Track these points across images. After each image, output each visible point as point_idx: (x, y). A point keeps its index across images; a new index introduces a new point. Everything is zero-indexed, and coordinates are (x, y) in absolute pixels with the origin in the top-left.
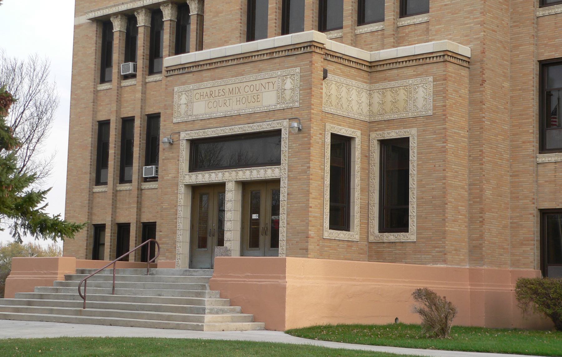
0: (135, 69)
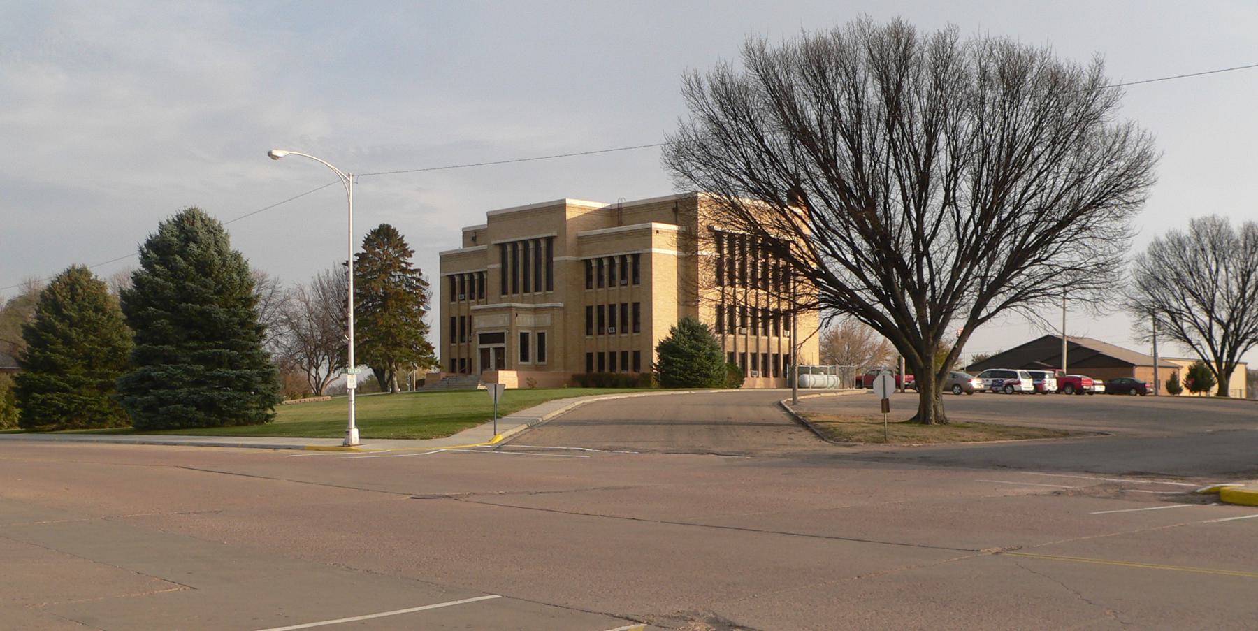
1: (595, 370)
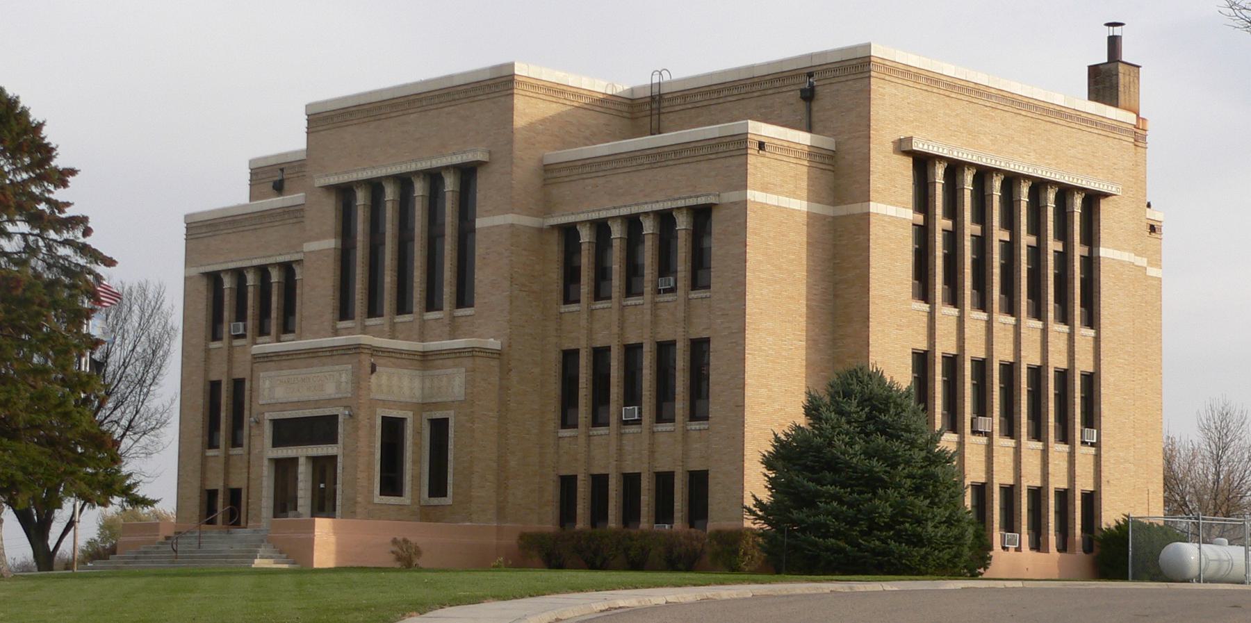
0: (245, 329)
1: (582, 523)
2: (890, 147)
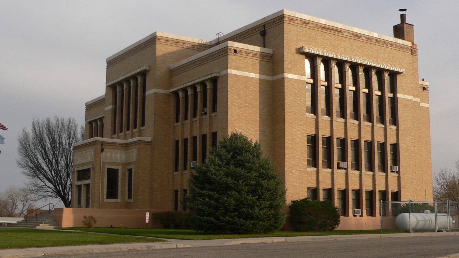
2: (294, 51)
